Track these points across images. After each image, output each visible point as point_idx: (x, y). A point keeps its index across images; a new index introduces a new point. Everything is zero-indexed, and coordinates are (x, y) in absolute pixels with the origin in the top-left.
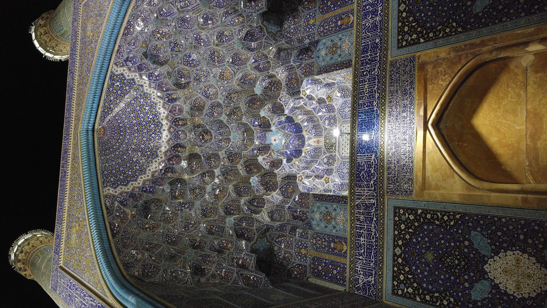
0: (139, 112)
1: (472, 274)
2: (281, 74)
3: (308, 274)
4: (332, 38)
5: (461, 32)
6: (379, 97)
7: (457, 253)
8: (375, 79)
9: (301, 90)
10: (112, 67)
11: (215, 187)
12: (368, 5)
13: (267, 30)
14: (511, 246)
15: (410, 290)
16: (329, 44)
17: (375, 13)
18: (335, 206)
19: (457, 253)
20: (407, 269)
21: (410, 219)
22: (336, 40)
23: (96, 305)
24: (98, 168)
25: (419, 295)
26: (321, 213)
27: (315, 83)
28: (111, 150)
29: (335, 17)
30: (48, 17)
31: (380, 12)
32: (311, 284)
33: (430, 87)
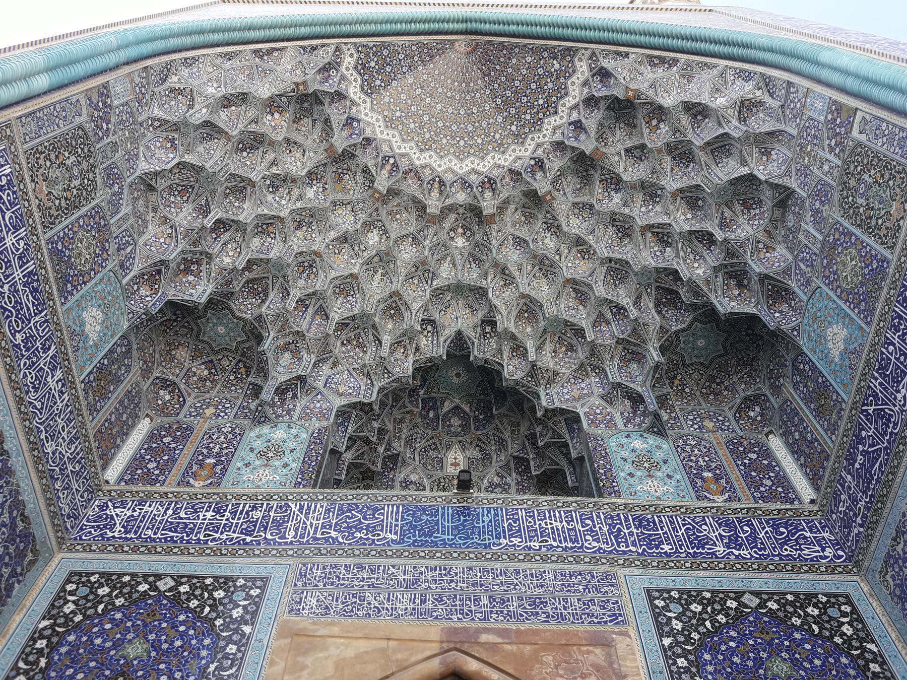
3: (158, 420)
6: (530, 548)
10: (586, 49)
11: (356, 249)
13: (682, 330)
16: (659, 456)
21: (233, 609)
24: (394, 38)
26: (285, 441)
29: (720, 467)
32: (135, 418)
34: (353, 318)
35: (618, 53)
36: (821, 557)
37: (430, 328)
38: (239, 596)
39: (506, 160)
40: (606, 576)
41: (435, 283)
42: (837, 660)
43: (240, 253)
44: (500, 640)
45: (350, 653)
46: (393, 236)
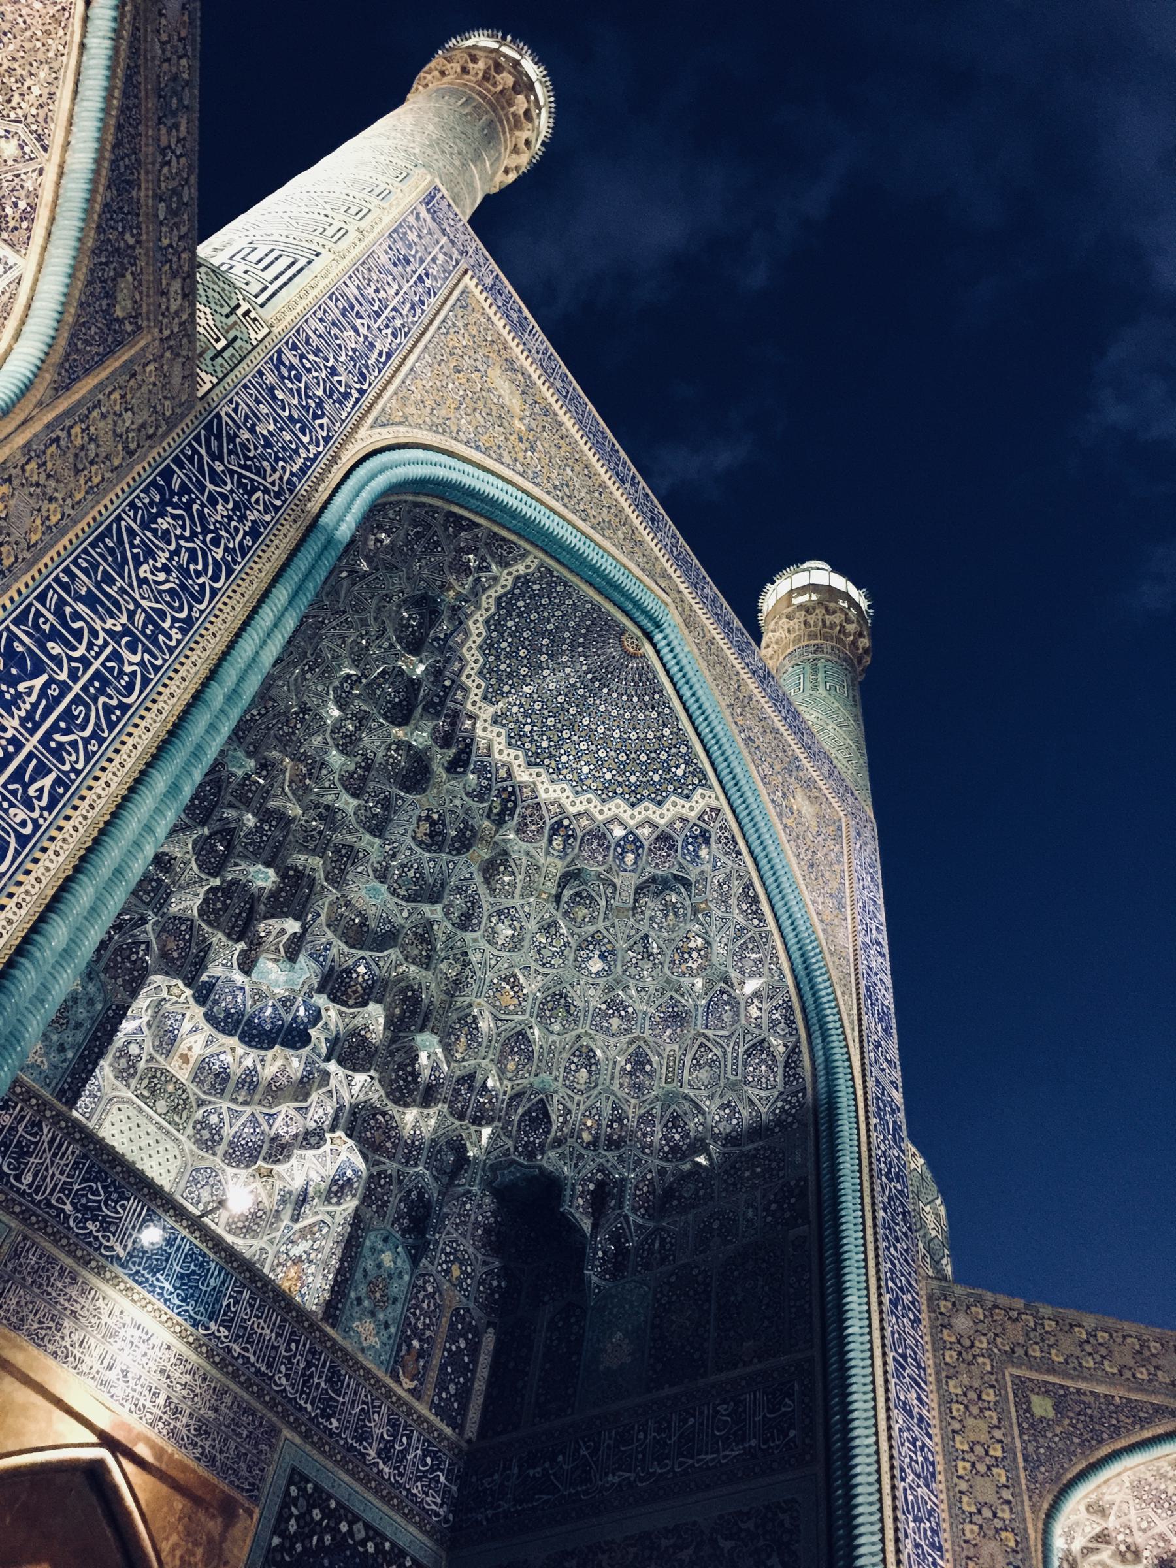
0: (593, 748)
2: (415, 1121)
6: (230, 1351)
8: (269, 1366)
9: (351, 1143)
10: (717, 798)
11: (324, 772)
12: (409, 1444)
13: (520, 1164)
16: (396, 1288)
18: (70, 1055)
24: (584, 587)
27: (334, 1182)
30: (860, 662)
31: (381, 1466)
33: (179, 1503)
35: (736, 843)
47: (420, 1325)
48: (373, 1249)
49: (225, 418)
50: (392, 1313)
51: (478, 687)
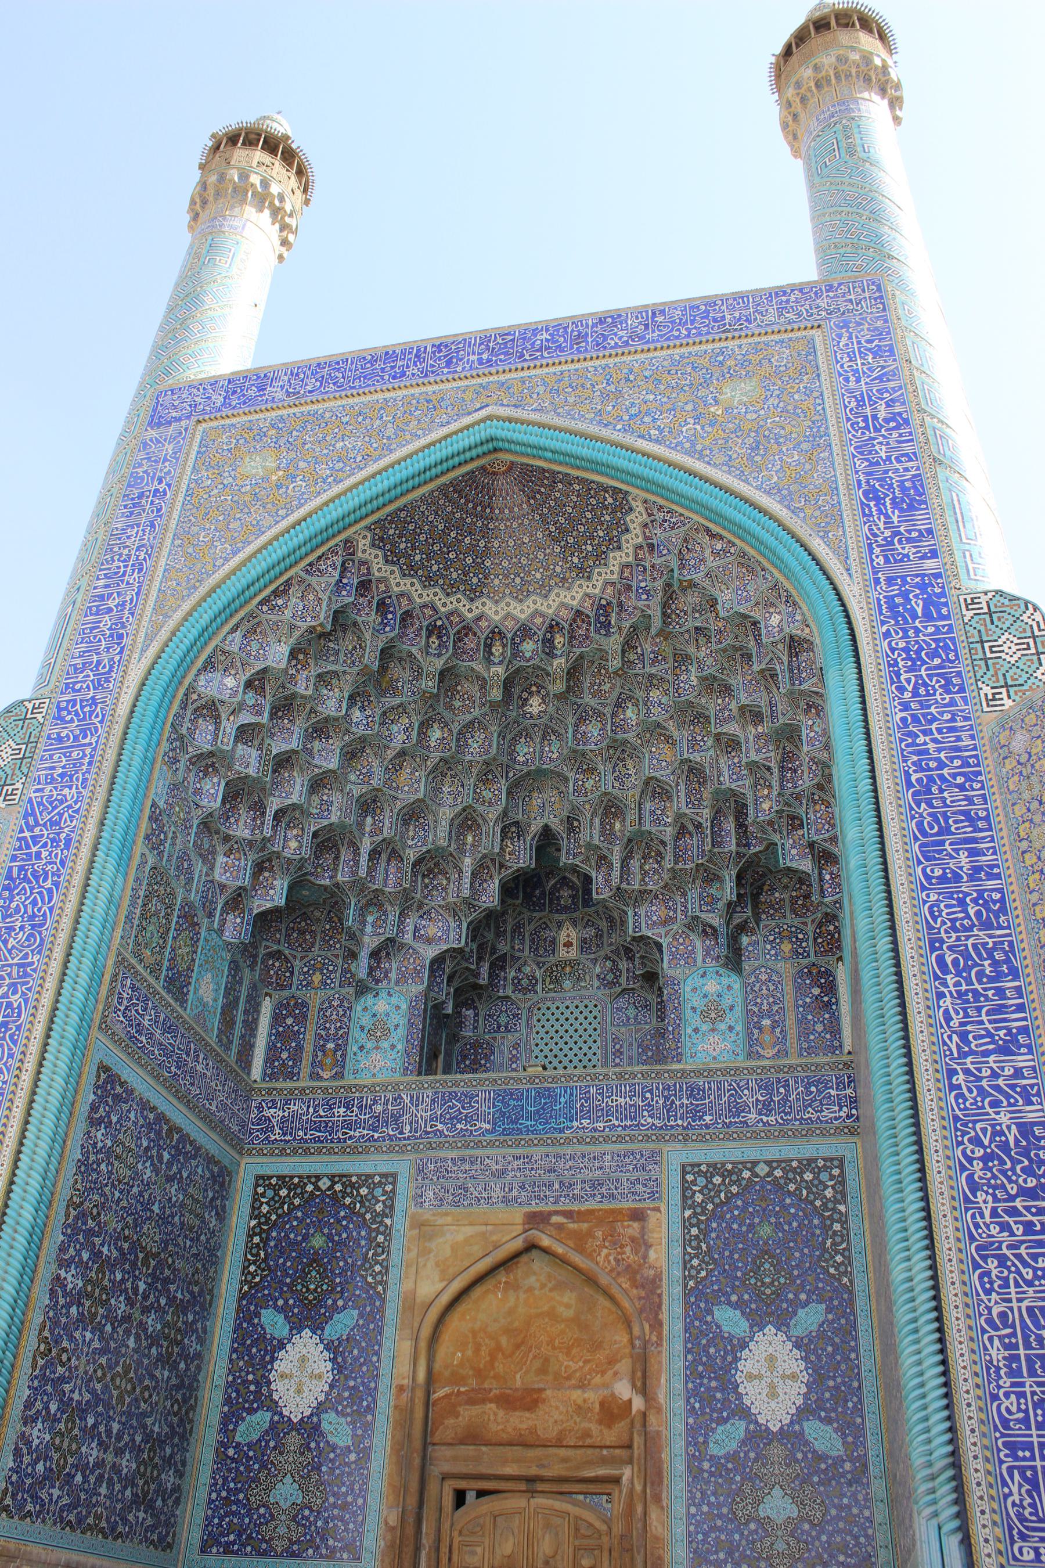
1: (296, 1310)
3: (277, 995)
4: (739, 1010)
5: (686, 1286)
6: (595, 1130)
7: (325, 1287)
14: (339, 1368)
15: (265, 1209)
16: (727, 1001)
17: (766, 1108)
18: (399, 1047)
19: (325, 1287)
20: (297, 1201)
22: (731, 1018)
23: (124, 627)
25: (259, 1224)
26: (388, 1015)
28: (463, 501)
31: (765, 1119)
34: (428, 851)
36: (836, 1119)
37: (513, 829)
38: (378, 1192)
39: (573, 598)
40: (653, 1153)
41: (511, 774)
42: (811, 1222)
43: (303, 829)
44: (565, 1221)
45: (460, 1237)
46: (456, 728)
47: (765, 1007)
48: (694, 990)
49: (33, 795)
50: (736, 1018)
51: (459, 601)
